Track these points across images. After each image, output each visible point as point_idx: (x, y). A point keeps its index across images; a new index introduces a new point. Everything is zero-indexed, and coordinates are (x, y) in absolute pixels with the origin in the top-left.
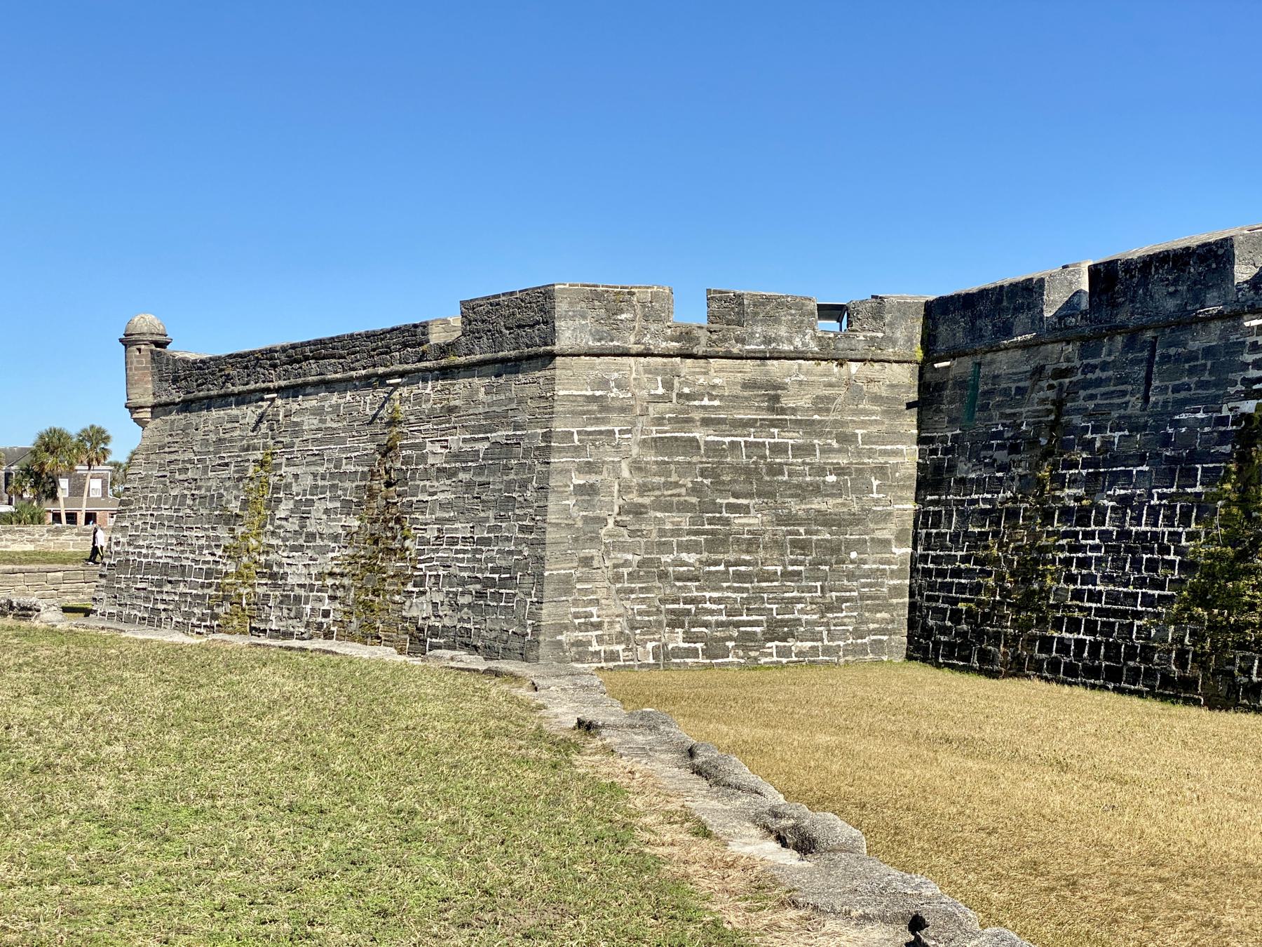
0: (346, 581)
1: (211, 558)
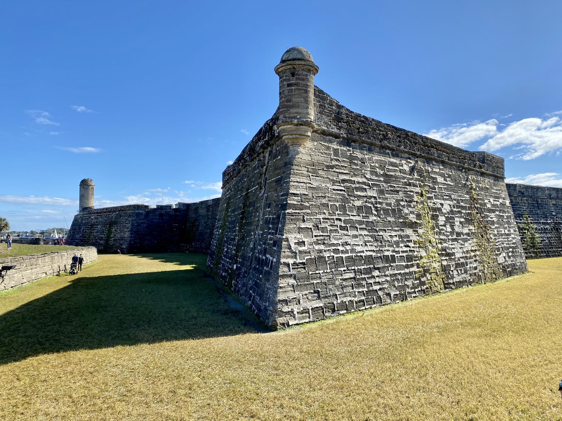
0: (478, 253)
1: (408, 249)
